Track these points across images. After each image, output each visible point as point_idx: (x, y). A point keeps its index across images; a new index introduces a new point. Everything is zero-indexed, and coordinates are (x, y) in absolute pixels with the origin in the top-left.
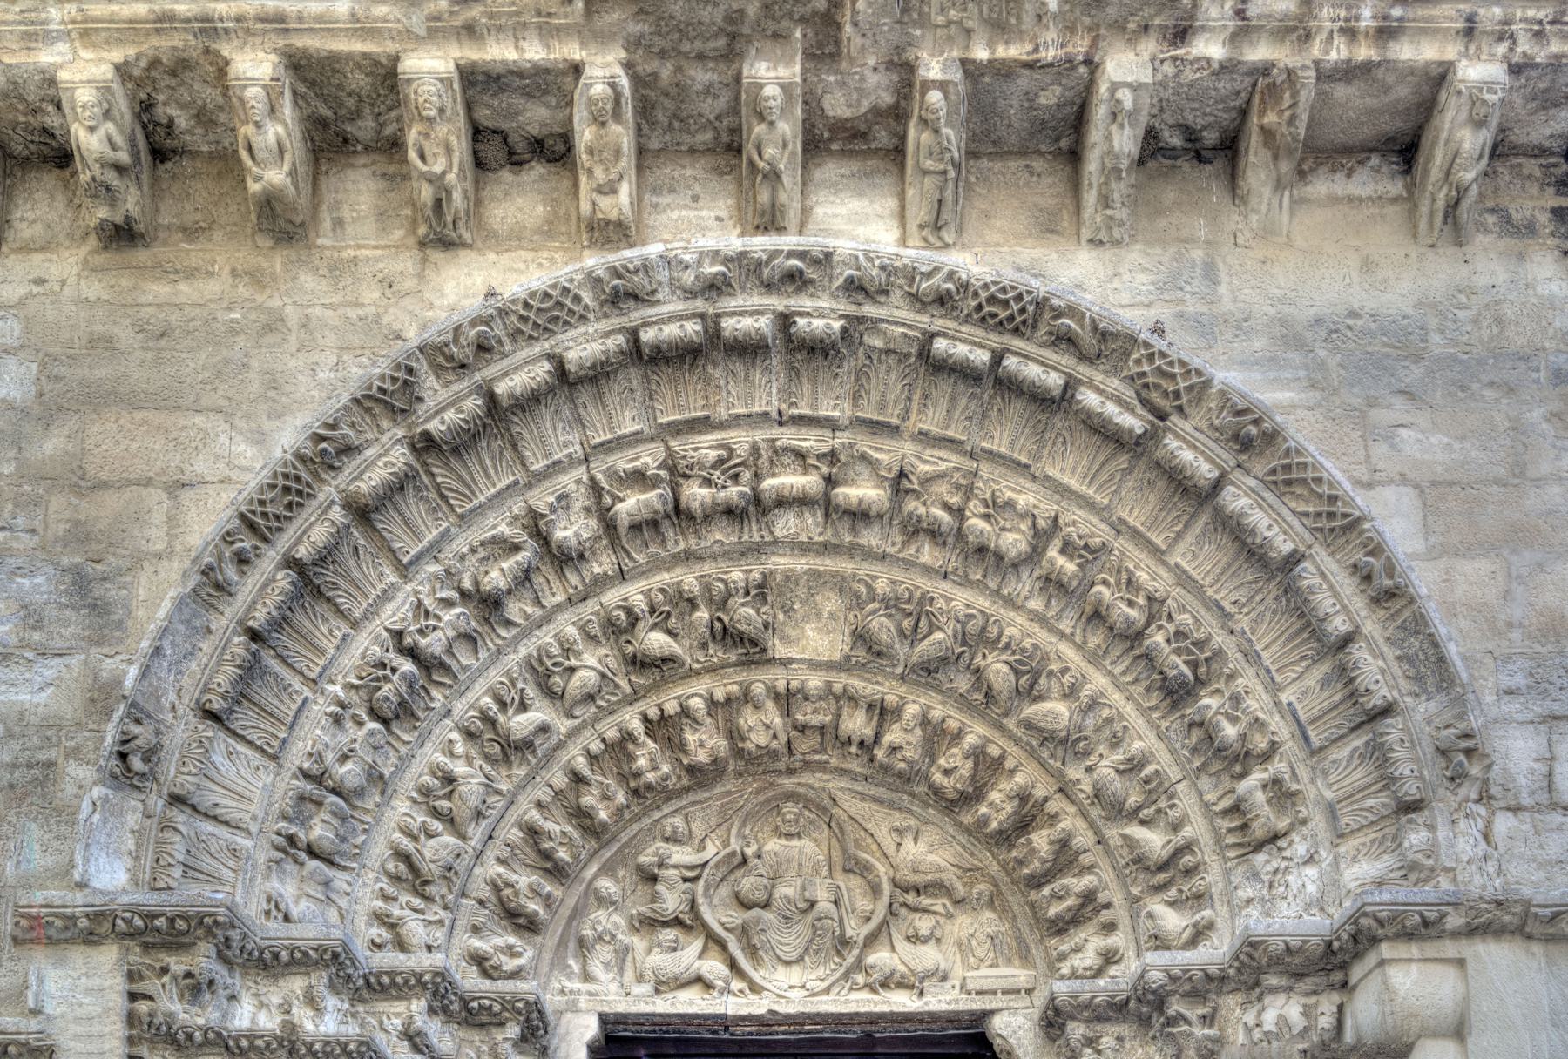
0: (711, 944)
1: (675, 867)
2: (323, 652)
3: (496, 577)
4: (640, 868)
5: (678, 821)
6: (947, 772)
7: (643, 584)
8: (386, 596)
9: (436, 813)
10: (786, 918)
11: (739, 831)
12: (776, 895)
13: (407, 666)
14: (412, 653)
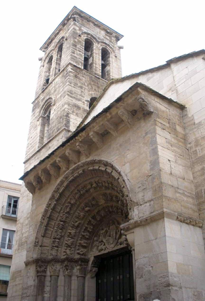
2: (53, 225)
3: (68, 210)
7: (83, 203)
8: (58, 216)
9: (70, 237)
13: (62, 223)
14: (62, 221)
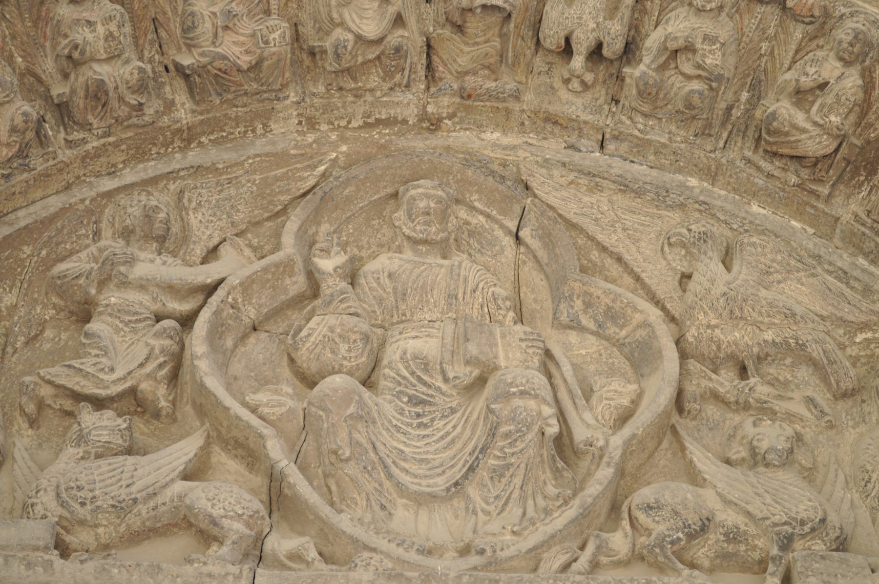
0: (220, 457)
1: (142, 286)
4: (61, 286)
5: (161, 199)
6: (801, 96)
10: (415, 401)
11: (302, 231)
12: (392, 354)
